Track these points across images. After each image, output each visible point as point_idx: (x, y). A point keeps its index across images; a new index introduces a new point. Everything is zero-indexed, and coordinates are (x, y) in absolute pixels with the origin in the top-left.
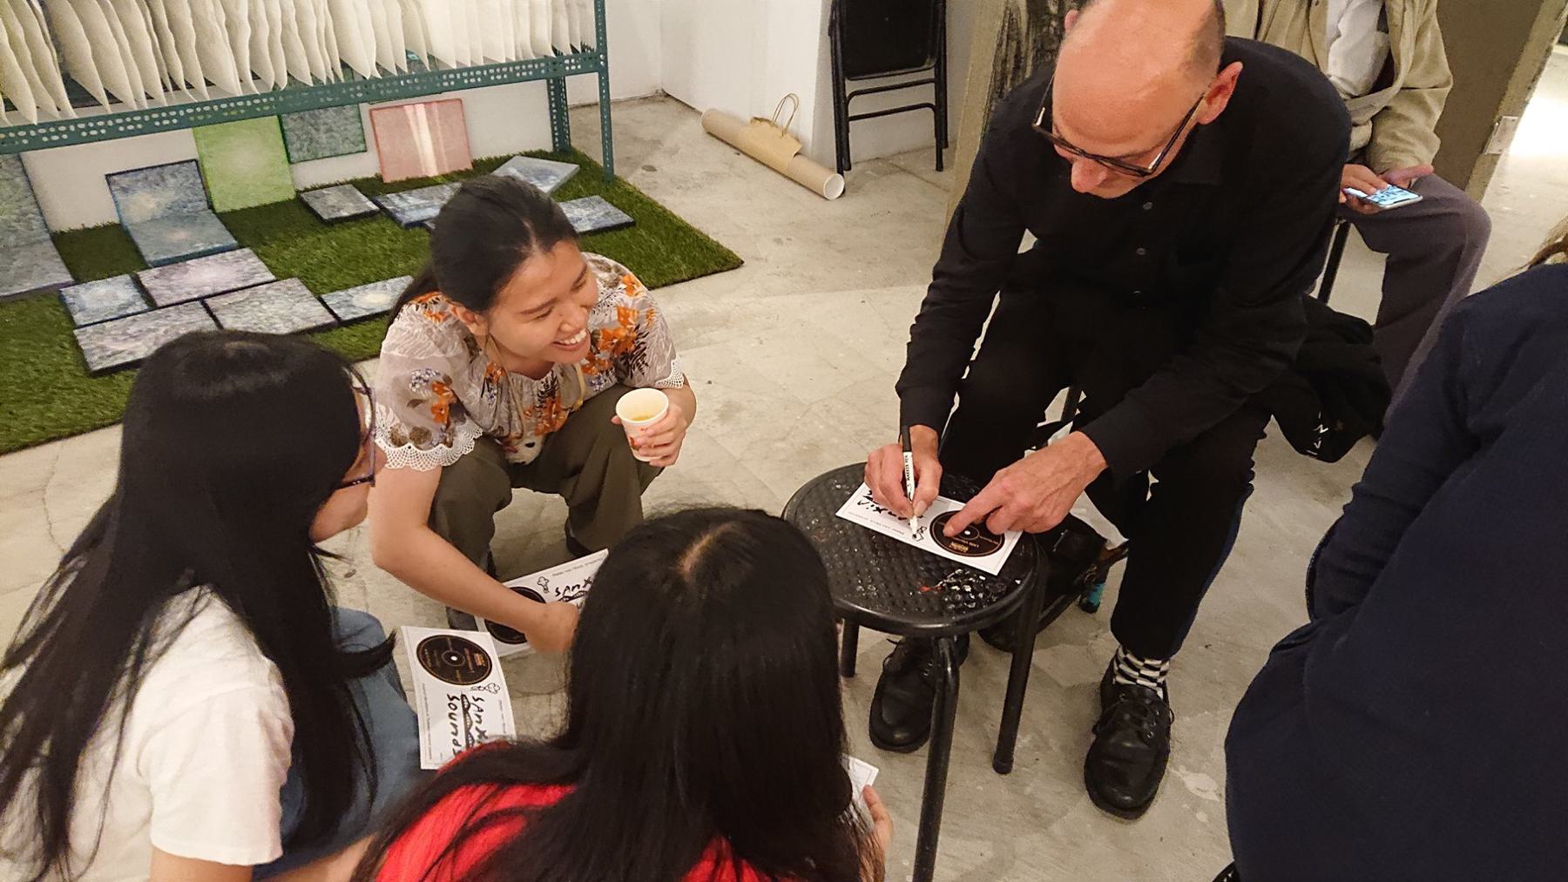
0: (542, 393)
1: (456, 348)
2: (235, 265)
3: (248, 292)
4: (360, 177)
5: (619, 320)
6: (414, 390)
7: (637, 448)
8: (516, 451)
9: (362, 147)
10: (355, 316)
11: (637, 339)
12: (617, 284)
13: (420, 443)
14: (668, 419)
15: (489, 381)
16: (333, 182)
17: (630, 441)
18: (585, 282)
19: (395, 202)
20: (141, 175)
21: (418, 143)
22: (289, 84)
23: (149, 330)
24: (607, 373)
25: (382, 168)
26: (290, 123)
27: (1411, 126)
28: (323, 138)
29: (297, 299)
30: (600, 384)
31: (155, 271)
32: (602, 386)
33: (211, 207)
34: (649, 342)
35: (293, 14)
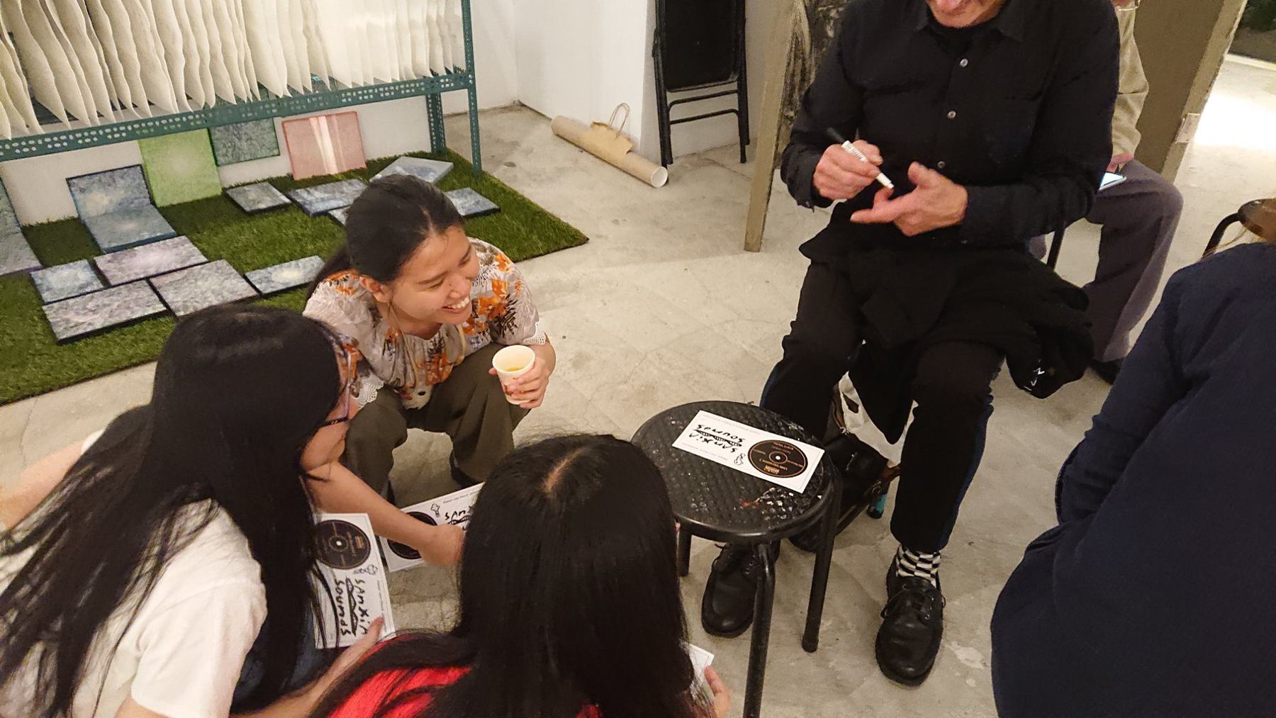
0: (431, 349)
1: (363, 315)
2: (174, 250)
3: (186, 271)
4: (274, 176)
5: (493, 290)
7: (510, 394)
8: (411, 399)
9: (276, 152)
11: (508, 305)
12: (491, 262)
15: (388, 341)
16: (252, 181)
17: (504, 388)
19: (303, 195)
20: (96, 178)
21: (321, 147)
22: (217, 103)
23: (105, 305)
24: (484, 333)
25: (293, 171)
26: (217, 134)
28: (244, 145)
29: (226, 277)
30: (478, 342)
31: (108, 257)
32: (480, 344)
33: (153, 203)
34: (517, 308)
35: (219, 47)
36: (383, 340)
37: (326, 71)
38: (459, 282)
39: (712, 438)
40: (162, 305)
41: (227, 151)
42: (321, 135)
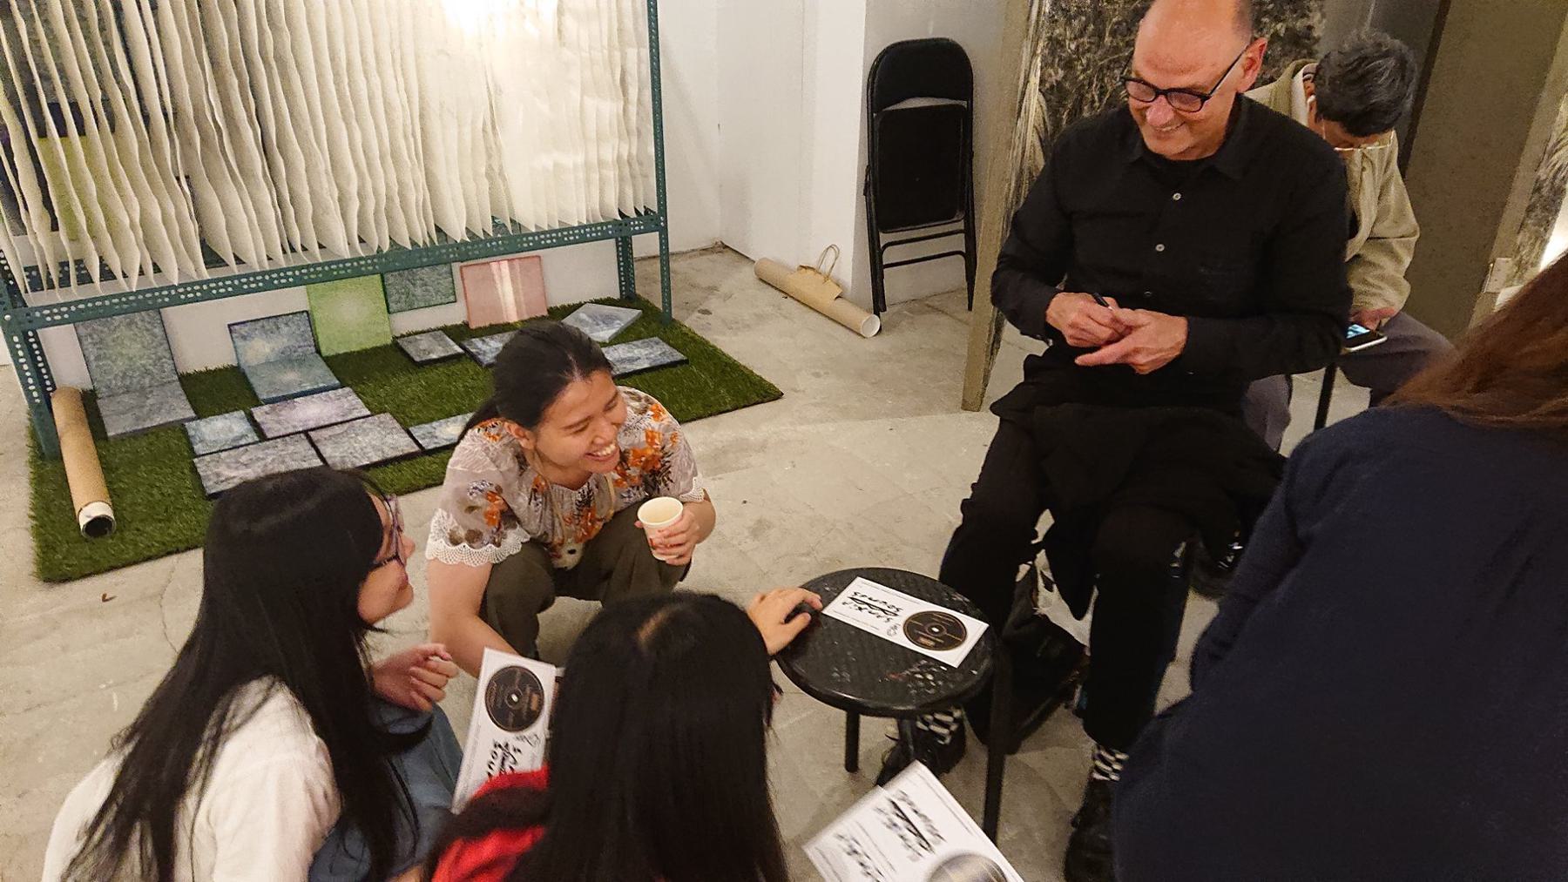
0: (579, 502)
1: (509, 463)
3: (347, 425)
4: (449, 324)
5: (647, 442)
6: (471, 498)
7: (655, 548)
8: (560, 557)
9: (452, 298)
10: (438, 446)
11: (663, 457)
12: (646, 411)
13: (473, 542)
14: (683, 522)
15: (535, 491)
16: (425, 329)
17: (649, 542)
18: (615, 405)
20: (260, 323)
22: (391, 246)
23: (258, 459)
24: (638, 489)
25: (469, 317)
26: (390, 279)
27: (1378, 272)
28: (419, 291)
30: (629, 497)
31: (266, 408)
32: (631, 499)
33: (318, 351)
34: (673, 461)
35: (396, 189)
36: (530, 490)
37: (478, 218)
38: (604, 429)
39: (866, 606)
40: (319, 460)
41: (400, 298)
42: (501, 278)
